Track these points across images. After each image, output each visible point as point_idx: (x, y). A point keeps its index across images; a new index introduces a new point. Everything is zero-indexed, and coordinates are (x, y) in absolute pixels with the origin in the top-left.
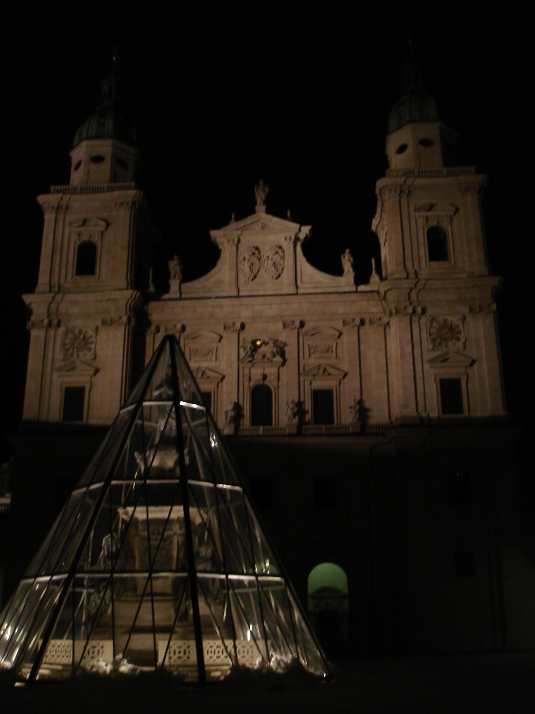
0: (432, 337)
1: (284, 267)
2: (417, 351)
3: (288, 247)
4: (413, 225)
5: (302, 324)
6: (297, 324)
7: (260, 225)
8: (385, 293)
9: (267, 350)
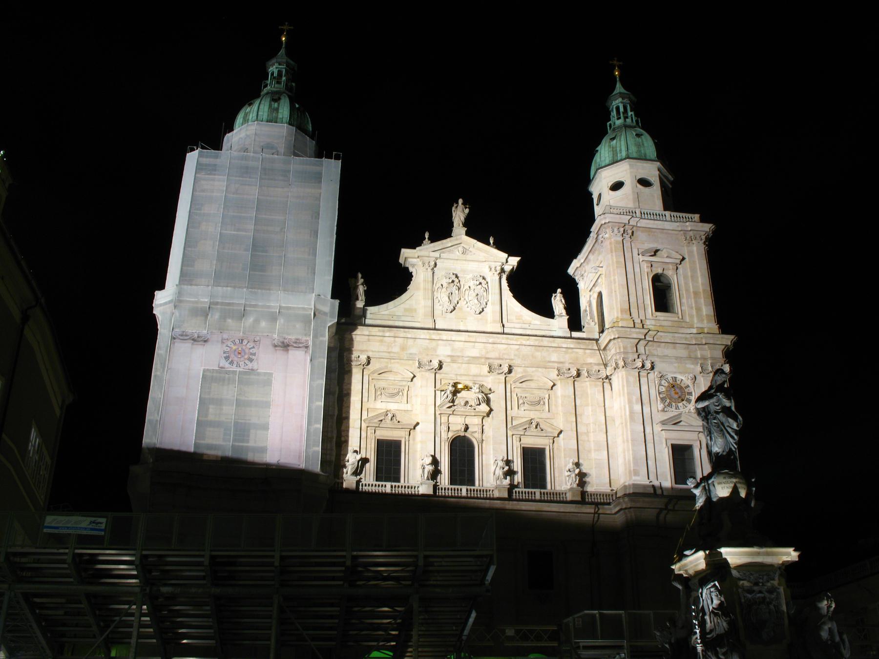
0: (661, 396)
1: (488, 301)
2: (647, 410)
3: (493, 278)
4: (637, 270)
5: (510, 371)
6: (506, 370)
7: (461, 249)
8: (610, 340)
9: (471, 396)
